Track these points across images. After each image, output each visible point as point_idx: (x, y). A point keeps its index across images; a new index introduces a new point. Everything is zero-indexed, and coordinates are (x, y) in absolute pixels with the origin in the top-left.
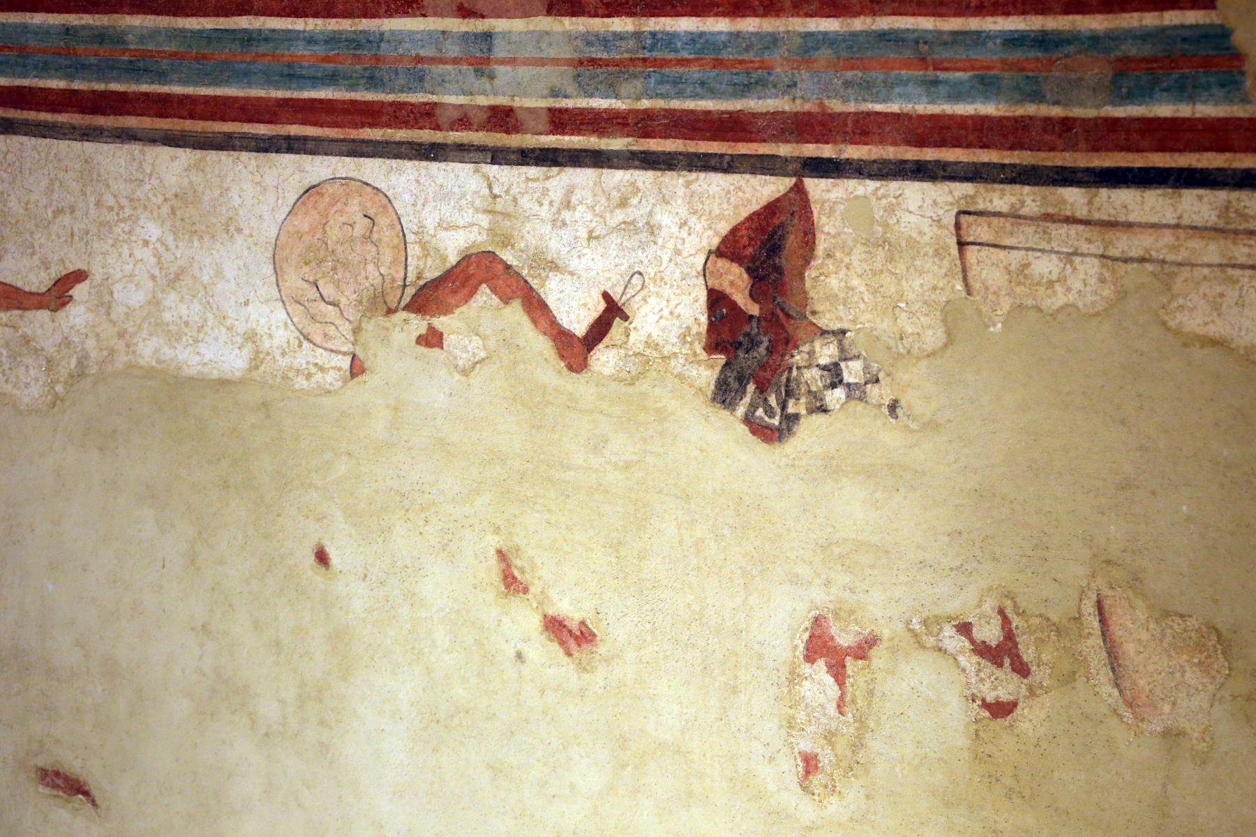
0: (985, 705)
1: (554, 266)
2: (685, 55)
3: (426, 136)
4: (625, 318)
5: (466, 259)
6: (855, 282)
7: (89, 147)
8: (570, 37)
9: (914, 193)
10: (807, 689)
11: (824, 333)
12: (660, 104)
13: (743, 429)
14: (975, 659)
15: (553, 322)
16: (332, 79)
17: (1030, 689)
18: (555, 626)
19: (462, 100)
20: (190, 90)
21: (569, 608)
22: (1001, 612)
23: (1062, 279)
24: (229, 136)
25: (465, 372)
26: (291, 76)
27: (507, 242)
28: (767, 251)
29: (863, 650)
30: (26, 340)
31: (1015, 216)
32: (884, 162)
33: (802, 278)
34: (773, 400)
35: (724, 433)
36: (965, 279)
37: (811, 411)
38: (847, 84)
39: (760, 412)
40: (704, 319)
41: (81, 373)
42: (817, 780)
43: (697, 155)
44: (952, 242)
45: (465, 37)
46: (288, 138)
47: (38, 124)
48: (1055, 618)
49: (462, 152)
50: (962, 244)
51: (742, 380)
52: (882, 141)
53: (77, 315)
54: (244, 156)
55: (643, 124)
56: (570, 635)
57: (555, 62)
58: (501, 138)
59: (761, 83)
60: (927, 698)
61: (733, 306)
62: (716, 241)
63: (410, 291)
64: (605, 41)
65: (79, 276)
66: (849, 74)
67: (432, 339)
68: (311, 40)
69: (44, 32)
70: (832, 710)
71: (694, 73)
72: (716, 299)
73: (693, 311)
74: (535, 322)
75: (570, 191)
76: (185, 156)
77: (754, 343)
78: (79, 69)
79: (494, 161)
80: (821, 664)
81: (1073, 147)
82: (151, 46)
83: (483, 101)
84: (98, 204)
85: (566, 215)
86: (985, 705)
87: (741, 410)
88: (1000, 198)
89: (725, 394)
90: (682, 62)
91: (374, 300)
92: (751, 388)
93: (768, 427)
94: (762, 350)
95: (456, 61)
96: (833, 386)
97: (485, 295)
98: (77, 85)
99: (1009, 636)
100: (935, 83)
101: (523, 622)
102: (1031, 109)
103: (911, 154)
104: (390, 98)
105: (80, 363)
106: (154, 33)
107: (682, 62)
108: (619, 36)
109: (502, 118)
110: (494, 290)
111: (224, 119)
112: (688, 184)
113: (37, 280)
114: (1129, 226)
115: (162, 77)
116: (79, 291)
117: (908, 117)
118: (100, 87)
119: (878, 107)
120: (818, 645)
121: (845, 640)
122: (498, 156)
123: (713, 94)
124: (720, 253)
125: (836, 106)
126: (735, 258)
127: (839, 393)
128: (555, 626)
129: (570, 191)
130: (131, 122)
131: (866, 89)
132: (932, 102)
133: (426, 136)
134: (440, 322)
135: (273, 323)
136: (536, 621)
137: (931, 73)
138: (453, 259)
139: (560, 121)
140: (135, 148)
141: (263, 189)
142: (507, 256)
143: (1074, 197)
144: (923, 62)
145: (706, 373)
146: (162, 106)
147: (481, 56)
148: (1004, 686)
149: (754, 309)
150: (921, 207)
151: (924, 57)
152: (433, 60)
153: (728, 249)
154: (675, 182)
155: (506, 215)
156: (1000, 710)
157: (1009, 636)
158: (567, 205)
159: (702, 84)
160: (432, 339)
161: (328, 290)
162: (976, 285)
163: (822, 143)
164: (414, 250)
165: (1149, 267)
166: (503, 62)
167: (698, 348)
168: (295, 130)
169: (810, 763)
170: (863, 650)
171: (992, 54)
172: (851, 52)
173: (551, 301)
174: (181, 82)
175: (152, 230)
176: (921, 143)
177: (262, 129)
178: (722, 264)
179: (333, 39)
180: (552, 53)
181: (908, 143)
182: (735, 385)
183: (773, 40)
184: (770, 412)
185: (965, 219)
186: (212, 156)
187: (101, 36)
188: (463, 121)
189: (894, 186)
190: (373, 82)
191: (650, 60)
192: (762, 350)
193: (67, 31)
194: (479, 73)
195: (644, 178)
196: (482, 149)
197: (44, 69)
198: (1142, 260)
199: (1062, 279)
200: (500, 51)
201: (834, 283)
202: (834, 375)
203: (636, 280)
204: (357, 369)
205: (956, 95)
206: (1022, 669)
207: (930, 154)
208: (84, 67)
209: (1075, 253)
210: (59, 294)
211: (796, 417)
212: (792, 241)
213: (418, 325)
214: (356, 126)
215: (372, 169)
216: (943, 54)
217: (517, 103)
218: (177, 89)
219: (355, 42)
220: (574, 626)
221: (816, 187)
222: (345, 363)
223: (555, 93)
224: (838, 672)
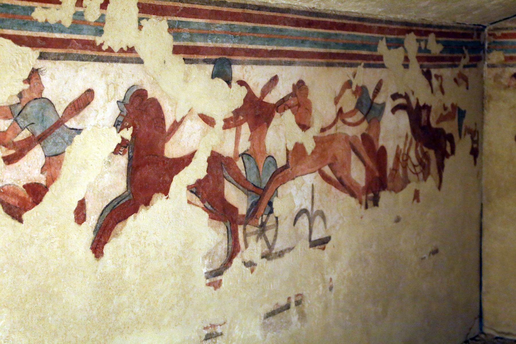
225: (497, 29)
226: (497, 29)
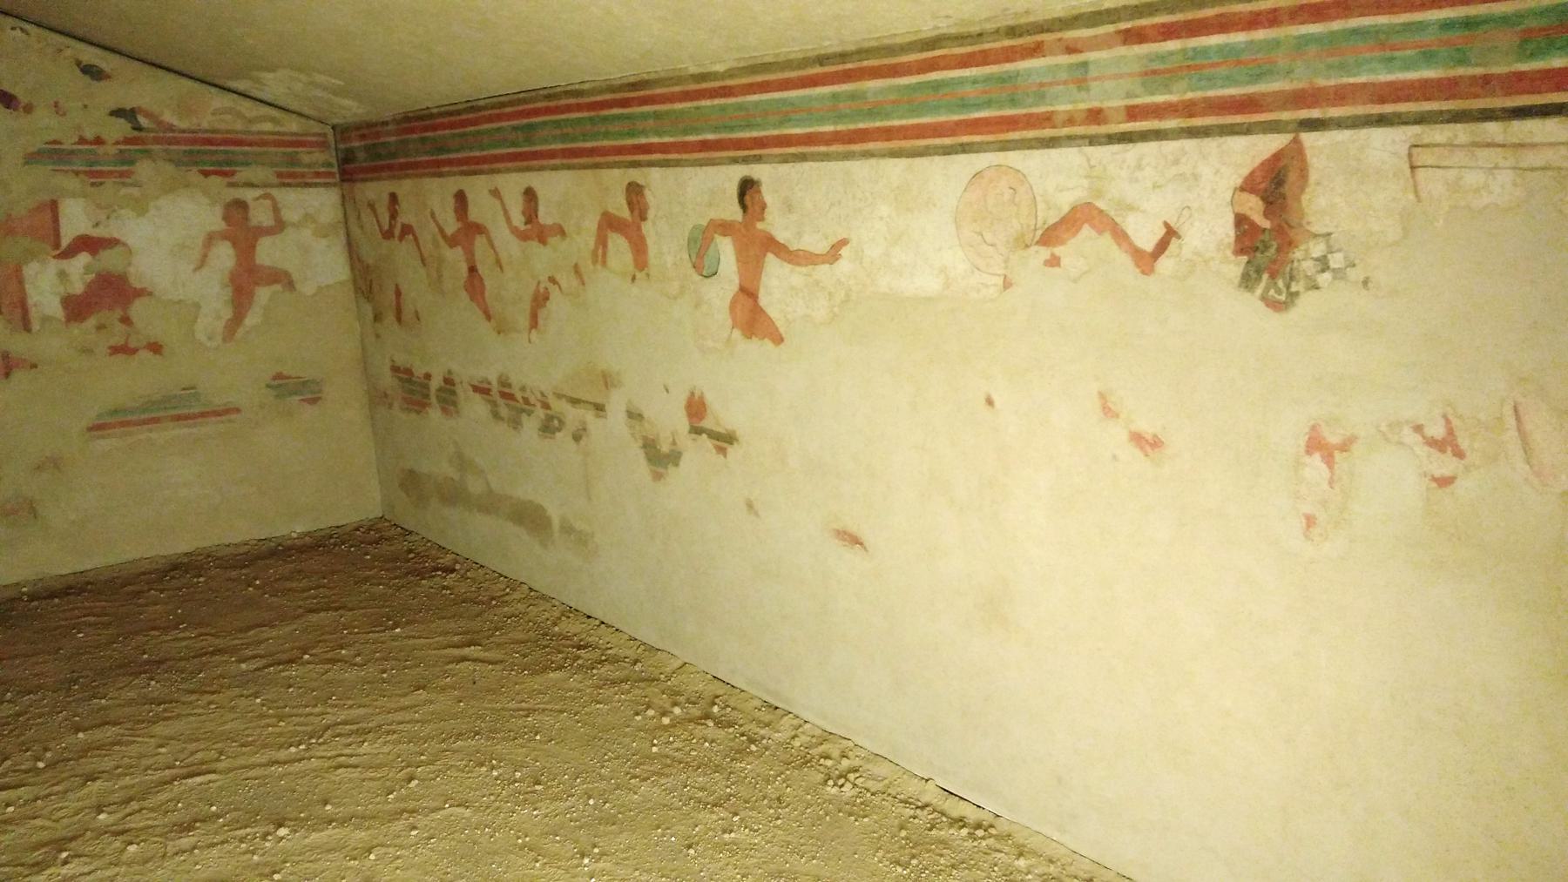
0: (1434, 479)
1: (1131, 208)
2: (1216, 60)
3: (1047, 133)
4: (1179, 237)
5: (1074, 209)
6: (1337, 200)
7: (848, 164)
8: (1139, 58)
9: (1378, 135)
10: (1307, 473)
11: (1316, 236)
12: (1199, 94)
13: (1261, 305)
14: (1426, 448)
15: (1131, 244)
16: (988, 104)
17: (1467, 469)
18: (1137, 438)
19: (1069, 107)
20: (904, 122)
21: (1146, 427)
22: (1445, 417)
23: (1486, 186)
24: (927, 147)
25: (1075, 281)
26: (964, 105)
27: (1099, 194)
28: (1275, 185)
29: (1345, 447)
30: (817, 283)
31: (1451, 145)
32: (1357, 117)
33: (1299, 200)
34: (1280, 283)
35: (1250, 304)
36: (1416, 192)
37: (1308, 289)
38: (1330, 67)
39: (1272, 292)
40: (1232, 233)
41: (847, 300)
42: (1315, 531)
43: (1226, 126)
44: (1406, 167)
45: (1071, 66)
46: (962, 145)
47: (819, 154)
48: (1482, 416)
49: (1071, 140)
50: (1413, 168)
51: (1259, 272)
52: (1354, 103)
53: (844, 265)
54: (937, 158)
55: (1189, 109)
56: (1147, 443)
57: (1130, 75)
58: (1096, 129)
59: (1271, 72)
60: (1392, 478)
61: (1253, 224)
62: (1239, 181)
63: (1039, 233)
64: (1162, 58)
65: (843, 242)
66: (1330, 60)
67: (1054, 262)
68: (975, 82)
69: (822, 98)
70: (1325, 486)
71: (1223, 71)
72: (1241, 220)
73: (1226, 230)
74: (1119, 245)
75: (1140, 159)
76: (903, 163)
77: (1267, 247)
78: (840, 118)
79: (1091, 144)
80: (1317, 457)
81: (1493, 94)
82: (880, 98)
83: (1083, 106)
84: (854, 197)
85: (1139, 174)
86: (1434, 479)
87: (1259, 291)
88: (1439, 134)
89: (1247, 281)
90: (1213, 65)
91: (1017, 240)
92: (1265, 276)
93: (1279, 302)
94: (1273, 250)
95: (1065, 83)
96: (1323, 271)
97: (1086, 231)
98: (840, 127)
99: (1451, 432)
100: (1391, 59)
101: (1116, 434)
102: (1461, 71)
103: (1376, 109)
104: (1024, 111)
105: (847, 295)
106: (882, 91)
107: (1213, 65)
108: (1171, 53)
109: (1095, 116)
110: (1093, 226)
111: (924, 137)
112: (1219, 146)
113: (821, 247)
114: (1533, 146)
115: (888, 116)
116: (844, 251)
117: (1373, 84)
118: (852, 127)
119: (1351, 80)
120: (1315, 444)
121: (1334, 439)
122: (1093, 141)
123: (1236, 83)
124: (1242, 189)
125: (1322, 82)
126: (1252, 191)
127: (1327, 276)
128: (1137, 438)
129: (1140, 159)
130: (871, 146)
131: (1343, 68)
132: (1390, 72)
133: (1047, 133)
134: (1058, 250)
135: (955, 259)
136: (1125, 436)
137: (1388, 54)
138: (1066, 209)
139: (1133, 113)
140: (873, 161)
141: (946, 177)
142: (1101, 204)
143: (1493, 129)
144: (1383, 46)
145: (1235, 267)
146: (888, 134)
147: (1081, 78)
148: (1445, 465)
149: (1266, 224)
150: (1385, 145)
151: (1382, 41)
152: (1051, 84)
153: (1248, 186)
154: (1211, 144)
155: (1099, 178)
156: (1444, 482)
157: (1451, 432)
158: (1139, 167)
159: (1228, 78)
160: (1054, 262)
161: (988, 236)
162: (1423, 195)
163: (1312, 109)
164: (1041, 206)
165: (1550, 173)
166: (1096, 79)
167: (1229, 253)
168: (965, 139)
169: (1310, 521)
170: (1345, 447)
171: (1429, 37)
172: (1330, 43)
173: (1130, 232)
174: (901, 118)
175: (884, 210)
176: (1382, 100)
177: (947, 141)
178: (1245, 196)
179: (988, 79)
180: (1125, 70)
181: (1373, 102)
182: (1254, 275)
183: (1276, 44)
184: (1279, 292)
185: (1415, 151)
186: (918, 161)
187: (853, 96)
188: (1071, 121)
189: (1364, 133)
190: (1013, 102)
191: (1192, 66)
192: (1273, 250)
193: (834, 96)
194: (1080, 89)
195: (1190, 144)
196: (1083, 137)
197: (821, 121)
198: (1543, 169)
199: (1486, 186)
200: (1093, 73)
201: (1322, 202)
202: (1323, 264)
203: (1186, 212)
204: (1007, 284)
205: (1408, 65)
206: (1459, 454)
207: (1388, 108)
208: (846, 116)
209: (1496, 167)
210: (833, 254)
211: (1297, 294)
212: (1292, 177)
213: (1044, 253)
214: (1002, 131)
215: (1013, 158)
216: (1396, 39)
217: (1106, 104)
218: (896, 123)
219: (1002, 79)
220: (1149, 437)
221: (1308, 138)
222: (1000, 281)
223: (1129, 95)
224: (1329, 461)
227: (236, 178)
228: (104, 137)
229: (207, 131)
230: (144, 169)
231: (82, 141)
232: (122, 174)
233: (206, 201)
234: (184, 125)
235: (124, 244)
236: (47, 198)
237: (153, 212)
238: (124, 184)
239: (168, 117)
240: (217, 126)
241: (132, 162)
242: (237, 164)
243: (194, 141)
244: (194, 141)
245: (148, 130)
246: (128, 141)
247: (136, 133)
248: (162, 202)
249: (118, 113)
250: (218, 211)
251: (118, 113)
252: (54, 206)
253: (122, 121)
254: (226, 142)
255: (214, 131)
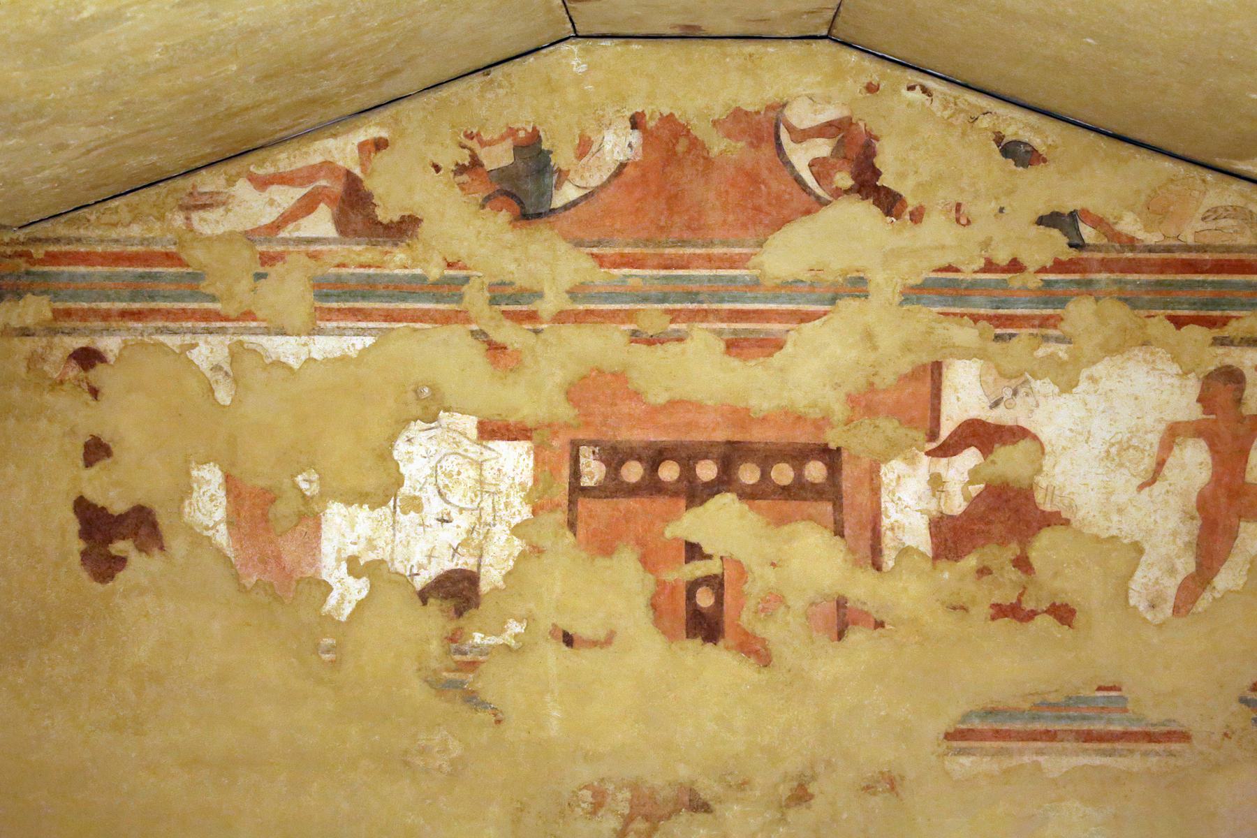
225: (36, 241)
226: (36, 241)
227: (1230, 330)
228: (1024, 258)
229: (1188, 249)
230: (1080, 313)
231: (990, 266)
232: (1044, 322)
233: (1175, 368)
234: (1153, 238)
235: (1035, 438)
236: (927, 359)
237: (1084, 385)
238: (1046, 339)
239: (1130, 225)
240: (1208, 239)
241: (1063, 303)
242: (1232, 305)
243: (1164, 267)
244: (1164, 267)
245: (1096, 248)
246: (1059, 266)
247: (1074, 253)
248: (1100, 369)
249: (1049, 220)
250: (1193, 387)
251: (1049, 220)
252: (936, 370)
253: (1056, 233)
254: (1219, 267)
255: (1203, 249)
